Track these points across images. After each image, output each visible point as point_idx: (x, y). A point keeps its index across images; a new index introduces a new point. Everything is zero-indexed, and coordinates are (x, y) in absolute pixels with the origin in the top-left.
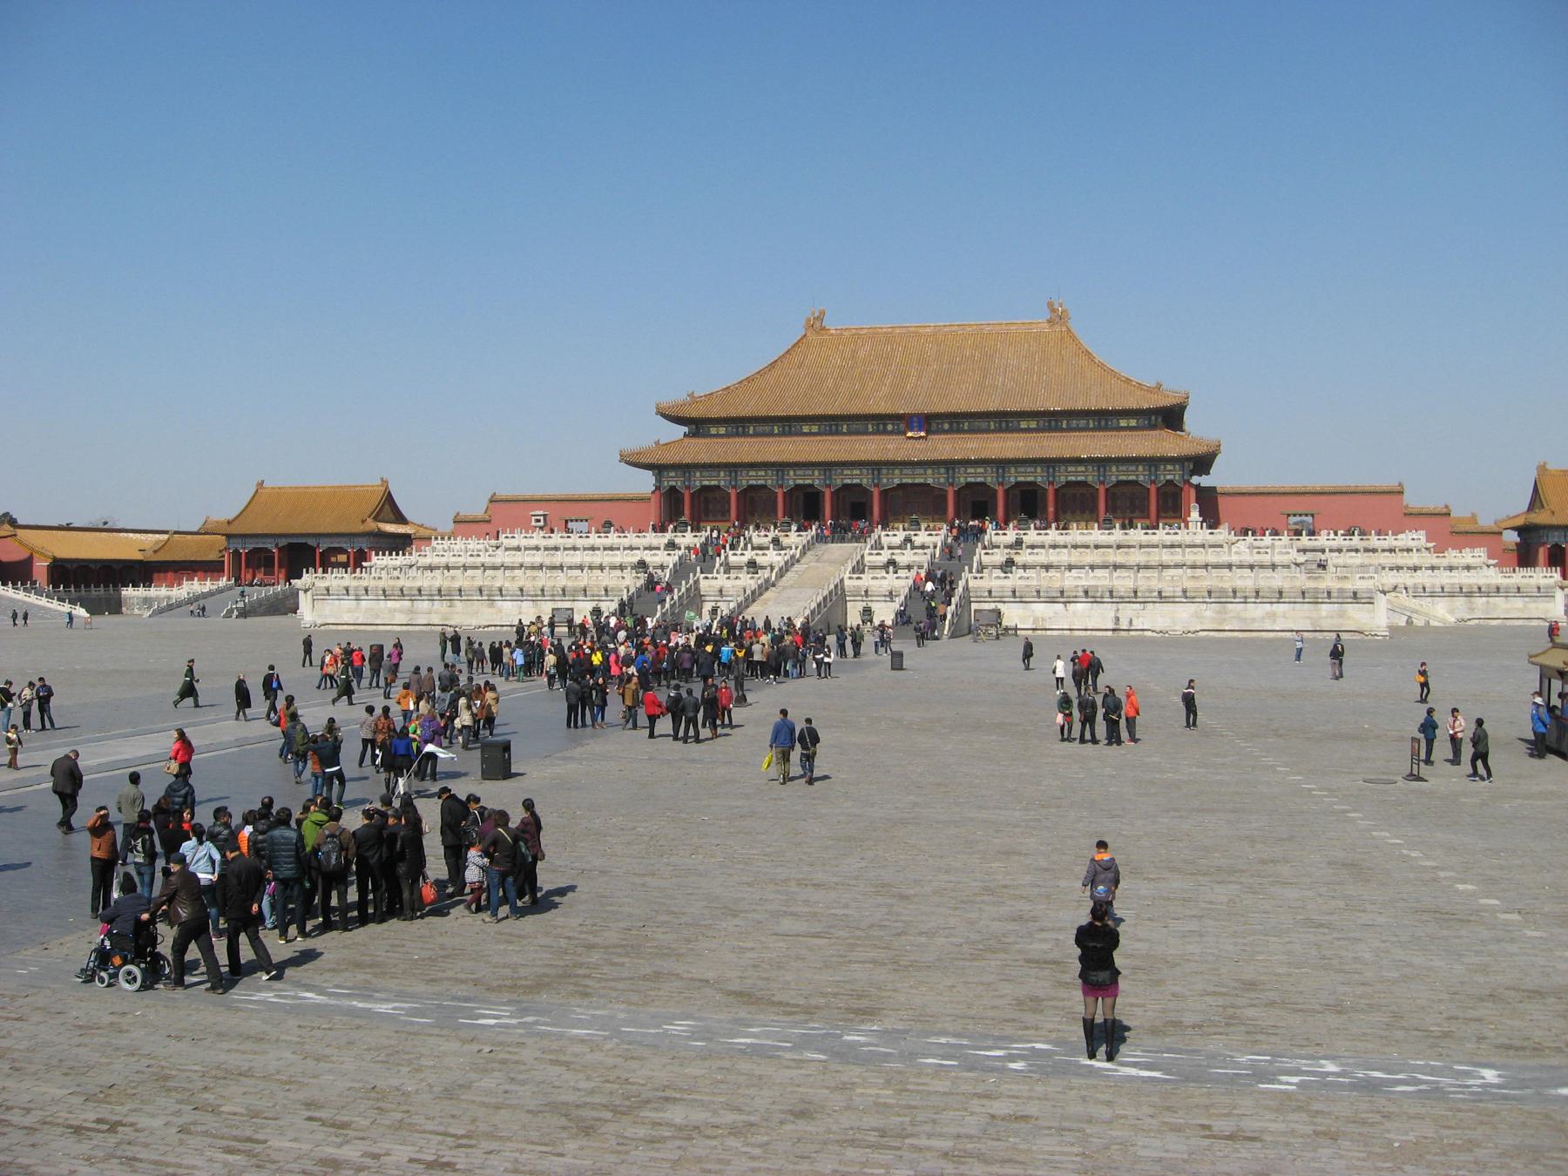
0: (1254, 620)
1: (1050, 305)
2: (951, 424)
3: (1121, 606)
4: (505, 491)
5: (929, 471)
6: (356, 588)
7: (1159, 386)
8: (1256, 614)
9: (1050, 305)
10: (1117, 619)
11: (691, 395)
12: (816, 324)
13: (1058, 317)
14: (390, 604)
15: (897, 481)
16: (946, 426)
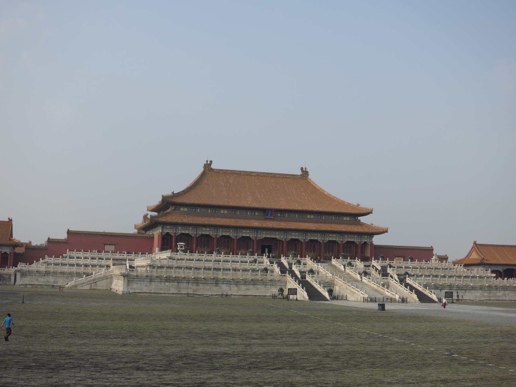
0: (500, 296)
1: (302, 169)
2: (281, 214)
3: (458, 291)
4: (73, 228)
5: (277, 233)
6: (151, 276)
7: (358, 205)
8: (500, 294)
9: (302, 169)
10: (458, 296)
11: (173, 193)
12: (208, 166)
13: (305, 173)
14: (167, 284)
15: (264, 236)
16: (279, 215)
